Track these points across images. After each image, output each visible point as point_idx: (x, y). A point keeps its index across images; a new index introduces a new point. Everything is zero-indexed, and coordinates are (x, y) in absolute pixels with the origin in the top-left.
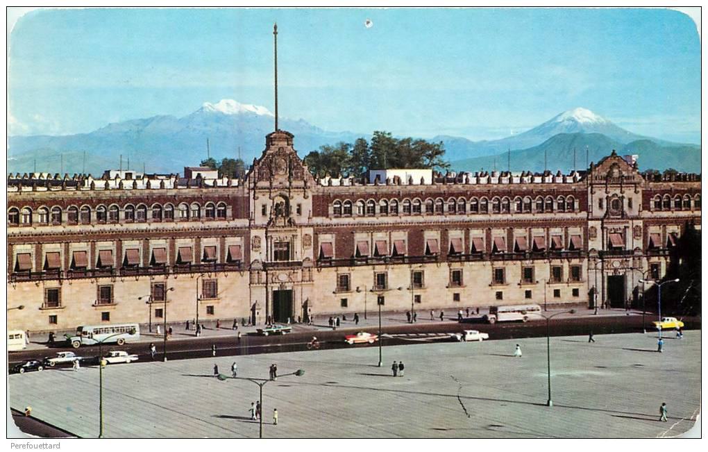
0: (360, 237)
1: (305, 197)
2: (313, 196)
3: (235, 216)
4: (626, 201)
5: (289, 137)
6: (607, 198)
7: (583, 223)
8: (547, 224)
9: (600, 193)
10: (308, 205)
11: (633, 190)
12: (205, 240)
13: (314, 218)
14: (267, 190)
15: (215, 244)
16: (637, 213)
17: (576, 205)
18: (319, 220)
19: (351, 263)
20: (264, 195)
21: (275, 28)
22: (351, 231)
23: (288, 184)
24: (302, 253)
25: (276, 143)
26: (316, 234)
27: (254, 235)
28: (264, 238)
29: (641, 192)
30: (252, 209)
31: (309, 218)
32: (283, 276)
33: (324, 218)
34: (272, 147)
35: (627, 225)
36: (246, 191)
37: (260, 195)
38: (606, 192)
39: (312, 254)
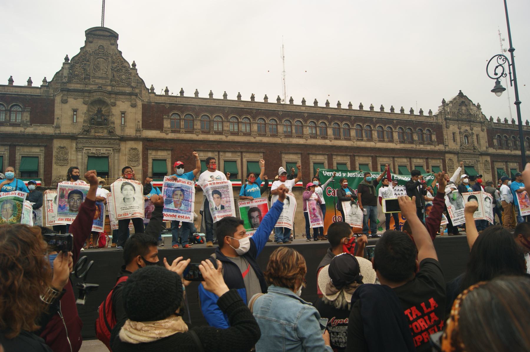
1: (134, 106)
2: (144, 106)
3: (35, 120)
4: (475, 137)
5: (113, 36)
6: (460, 133)
7: (441, 154)
8: (410, 154)
9: (453, 128)
10: (135, 116)
11: (479, 129)
14: (80, 94)
16: (484, 148)
17: (434, 137)
26: (145, 150)
27: (59, 145)
28: (74, 149)
29: (485, 130)
30: (57, 112)
33: (159, 132)
34: (91, 45)
35: (477, 159)
36: (51, 91)
37: (71, 101)
38: (459, 128)
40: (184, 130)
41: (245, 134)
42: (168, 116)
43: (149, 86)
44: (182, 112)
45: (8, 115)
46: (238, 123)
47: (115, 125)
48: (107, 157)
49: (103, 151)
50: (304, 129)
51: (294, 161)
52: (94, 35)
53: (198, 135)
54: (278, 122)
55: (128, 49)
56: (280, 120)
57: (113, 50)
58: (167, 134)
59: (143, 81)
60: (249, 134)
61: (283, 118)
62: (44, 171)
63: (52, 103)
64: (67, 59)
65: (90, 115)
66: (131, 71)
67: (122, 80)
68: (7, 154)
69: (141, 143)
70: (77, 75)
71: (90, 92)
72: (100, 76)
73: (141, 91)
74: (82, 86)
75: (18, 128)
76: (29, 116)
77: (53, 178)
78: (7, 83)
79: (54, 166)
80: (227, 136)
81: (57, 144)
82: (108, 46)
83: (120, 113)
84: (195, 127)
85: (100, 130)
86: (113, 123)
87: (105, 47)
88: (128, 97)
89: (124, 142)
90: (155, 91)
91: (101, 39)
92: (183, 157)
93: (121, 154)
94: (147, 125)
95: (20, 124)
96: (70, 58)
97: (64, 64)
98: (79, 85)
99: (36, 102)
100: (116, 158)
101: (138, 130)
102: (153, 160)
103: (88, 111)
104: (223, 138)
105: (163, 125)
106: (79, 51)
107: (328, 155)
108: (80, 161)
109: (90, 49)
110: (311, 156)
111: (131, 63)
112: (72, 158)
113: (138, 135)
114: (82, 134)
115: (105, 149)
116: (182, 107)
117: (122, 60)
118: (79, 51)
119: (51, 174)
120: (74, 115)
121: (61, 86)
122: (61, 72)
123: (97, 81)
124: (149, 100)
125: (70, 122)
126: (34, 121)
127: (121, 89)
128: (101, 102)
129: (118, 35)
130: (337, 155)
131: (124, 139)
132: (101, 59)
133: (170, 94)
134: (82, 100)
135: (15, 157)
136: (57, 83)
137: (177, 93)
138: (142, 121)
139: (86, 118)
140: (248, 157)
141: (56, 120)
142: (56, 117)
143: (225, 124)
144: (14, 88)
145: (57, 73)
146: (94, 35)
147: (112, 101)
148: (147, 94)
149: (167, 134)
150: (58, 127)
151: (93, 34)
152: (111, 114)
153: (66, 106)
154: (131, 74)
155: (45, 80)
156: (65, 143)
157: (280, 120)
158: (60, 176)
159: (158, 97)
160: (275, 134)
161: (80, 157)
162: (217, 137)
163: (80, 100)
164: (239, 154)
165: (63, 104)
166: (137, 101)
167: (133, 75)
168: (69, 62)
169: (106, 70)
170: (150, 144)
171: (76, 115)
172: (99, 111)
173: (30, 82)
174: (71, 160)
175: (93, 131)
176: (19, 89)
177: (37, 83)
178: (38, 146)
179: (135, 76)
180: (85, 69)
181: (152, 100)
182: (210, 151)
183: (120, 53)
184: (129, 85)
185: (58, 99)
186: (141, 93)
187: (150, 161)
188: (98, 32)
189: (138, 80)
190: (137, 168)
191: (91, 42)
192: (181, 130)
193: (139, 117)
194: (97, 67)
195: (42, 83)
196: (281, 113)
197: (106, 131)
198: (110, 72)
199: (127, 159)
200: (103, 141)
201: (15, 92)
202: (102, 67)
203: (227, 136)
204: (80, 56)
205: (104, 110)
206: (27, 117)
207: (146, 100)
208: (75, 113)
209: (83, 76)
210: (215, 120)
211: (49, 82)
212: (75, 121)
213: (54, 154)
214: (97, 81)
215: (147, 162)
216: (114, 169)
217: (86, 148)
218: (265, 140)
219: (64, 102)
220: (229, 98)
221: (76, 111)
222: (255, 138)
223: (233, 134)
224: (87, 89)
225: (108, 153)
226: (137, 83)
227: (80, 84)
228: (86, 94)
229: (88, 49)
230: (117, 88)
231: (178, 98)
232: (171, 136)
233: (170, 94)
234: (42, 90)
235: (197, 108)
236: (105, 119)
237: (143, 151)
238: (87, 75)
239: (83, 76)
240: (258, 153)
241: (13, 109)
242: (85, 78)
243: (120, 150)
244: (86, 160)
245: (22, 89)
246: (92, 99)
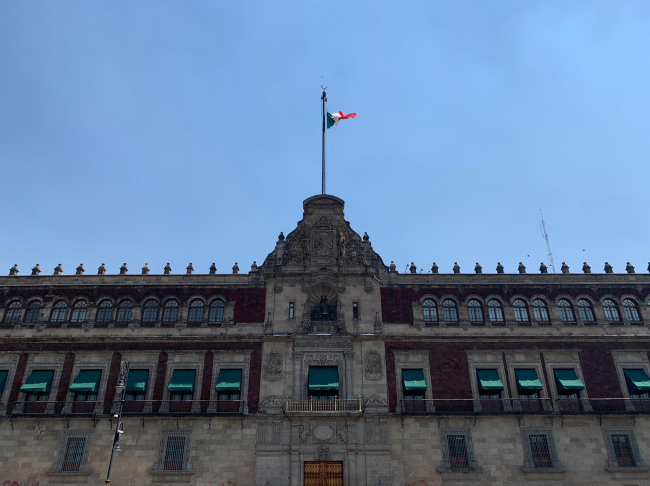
0: (476, 360)
1: (369, 290)
2: (382, 290)
10: (372, 304)
12: (177, 359)
13: (386, 326)
15: (193, 366)
18: (398, 329)
19: (466, 410)
20: (292, 286)
21: (324, 94)
22: (462, 348)
23: (335, 269)
24: (365, 385)
25: (316, 211)
27: (270, 350)
28: (290, 356)
30: (269, 305)
31: (375, 326)
32: (323, 432)
36: (262, 278)
39: (385, 389)
40: (444, 323)
41: (542, 324)
42: (419, 304)
43: (387, 263)
44: (439, 297)
45: (207, 313)
46: (527, 307)
47: (346, 319)
48: (336, 367)
49: (331, 359)
50: (643, 312)
51: (636, 366)
52: (314, 205)
53: (466, 330)
54: (593, 303)
55: (358, 218)
56: (597, 300)
57: (339, 221)
58: (420, 329)
59: (378, 255)
60: (549, 323)
61: (600, 296)
62: (249, 391)
63: (263, 293)
64: (281, 237)
65: (311, 307)
66: (363, 245)
67: (351, 258)
68: (200, 366)
69: (383, 343)
70: (294, 256)
71: (310, 275)
72: (324, 254)
73: (377, 270)
74: (300, 269)
75: (218, 329)
76: (233, 312)
77: (260, 401)
78: (208, 272)
79: (263, 383)
80: (512, 329)
81: (267, 348)
82: (332, 217)
83: (351, 303)
84: (461, 317)
85: (325, 327)
86: (343, 316)
87: (328, 219)
88: (361, 278)
89: (359, 343)
90: (396, 270)
91: (323, 209)
92: (448, 364)
93: (354, 362)
94: (389, 317)
95: (221, 325)
96: (286, 235)
97: (278, 243)
98: (297, 269)
100: (349, 367)
101: (377, 325)
102: (403, 370)
103: (308, 301)
104: (507, 331)
105: (412, 316)
106: (296, 226)
108: (298, 373)
109: (309, 223)
111: (362, 236)
112: (287, 370)
113: (377, 331)
114: (302, 334)
115: (333, 354)
116: (437, 289)
117: (351, 232)
118: (296, 226)
119: (258, 394)
120: (290, 307)
121: (274, 271)
122: (274, 254)
123: (319, 261)
124: (389, 282)
125: (286, 317)
126: (239, 319)
127: (351, 269)
128: (325, 287)
129: (344, 202)
131: (356, 337)
132: (324, 234)
133: (418, 271)
134: (301, 287)
135: (211, 370)
136: (269, 267)
137: (428, 270)
138: (382, 312)
139: (306, 312)
140: (555, 360)
141: (266, 317)
142: (267, 312)
143: (506, 310)
144: (216, 278)
145: (270, 255)
146: (314, 205)
147: (340, 285)
148: (387, 273)
149: (420, 329)
150: (270, 325)
151: (310, 204)
152: (339, 304)
153: (280, 297)
154: (362, 249)
155: (254, 266)
156: (279, 347)
157: (597, 300)
158: (270, 397)
159: (402, 278)
160: (594, 323)
161: (298, 367)
162: (498, 331)
163: (298, 287)
164: (538, 356)
165: (277, 295)
166: (374, 284)
167: (366, 250)
168: (285, 240)
169: (330, 247)
170: (394, 346)
171: (291, 307)
172: (324, 300)
173: (236, 269)
174: (286, 372)
175: (315, 329)
176: (223, 278)
177: (245, 269)
178: (243, 353)
179: (368, 252)
180: (303, 247)
181: (393, 282)
182: (489, 353)
183: (348, 223)
184: (360, 263)
185: (270, 288)
186: (377, 274)
187: (398, 372)
188: (319, 201)
189: (372, 256)
190: (379, 382)
191: (311, 214)
192: (441, 323)
193: (378, 306)
194: (319, 244)
195: (250, 269)
196: (595, 289)
197: (332, 328)
198: (336, 249)
199: (364, 369)
200: (328, 341)
201: (218, 282)
202: (325, 244)
203: (512, 329)
204: (297, 232)
205: (330, 298)
206: (229, 313)
207: (386, 282)
208: (292, 305)
209: (302, 256)
210: (489, 304)
211: (259, 267)
212: (291, 317)
213: (263, 363)
214: (319, 261)
215: (394, 373)
216: (346, 385)
217: (306, 354)
218: (576, 332)
219: (277, 290)
220: (506, 271)
221: (293, 303)
222: (558, 329)
223: (522, 324)
224: (306, 272)
225: (337, 361)
226: (372, 260)
227: (298, 266)
228: (306, 278)
229: (307, 223)
230: (346, 269)
231: (430, 277)
232: (426, 331)
233: (418, 271)
234: (250, 277)
235: (460, 289)
236: (332, 312)
237: (387, 357)
238: (307, 254)
239: (302, 256)
241: (213, 305)
242: (304, 259)
243: (353, 354)
244: (306, 372)
245: (226, 278)
246: (313, 284)
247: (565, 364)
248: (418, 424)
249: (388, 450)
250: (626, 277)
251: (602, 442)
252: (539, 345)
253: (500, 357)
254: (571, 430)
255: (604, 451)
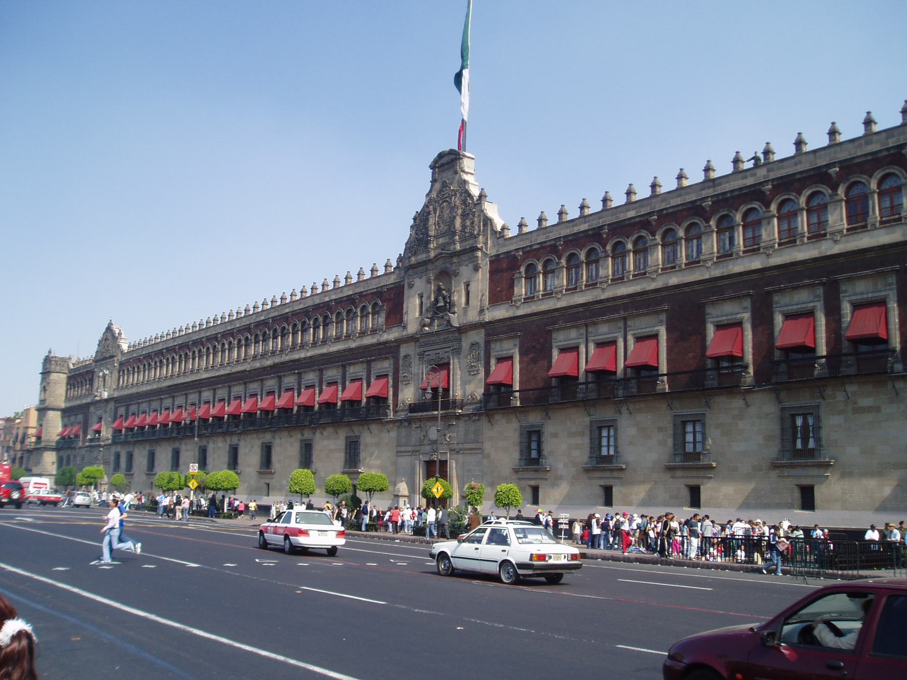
10: (481, 282)
69: (483, 330)
81: (404, 350)
99: (385, 297)
107: (823, 284)
110: (776, 298)
130: (850, 279)
147: (454, 268)
150: (405, 327)
178: (387, 358)
182: (573, 327)
188: (444, 160)
219: (411, 286)
240: (657, 313)
247: (647, 330)
248: (504, 421)
249: (480, 449)
250: (753, 171)
251: (671, 432)
252: (625, 307)
253: (583, 331)
254: (640, 417)
255: (670, 442)
